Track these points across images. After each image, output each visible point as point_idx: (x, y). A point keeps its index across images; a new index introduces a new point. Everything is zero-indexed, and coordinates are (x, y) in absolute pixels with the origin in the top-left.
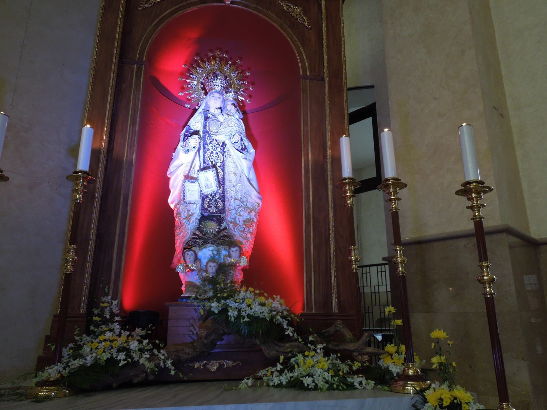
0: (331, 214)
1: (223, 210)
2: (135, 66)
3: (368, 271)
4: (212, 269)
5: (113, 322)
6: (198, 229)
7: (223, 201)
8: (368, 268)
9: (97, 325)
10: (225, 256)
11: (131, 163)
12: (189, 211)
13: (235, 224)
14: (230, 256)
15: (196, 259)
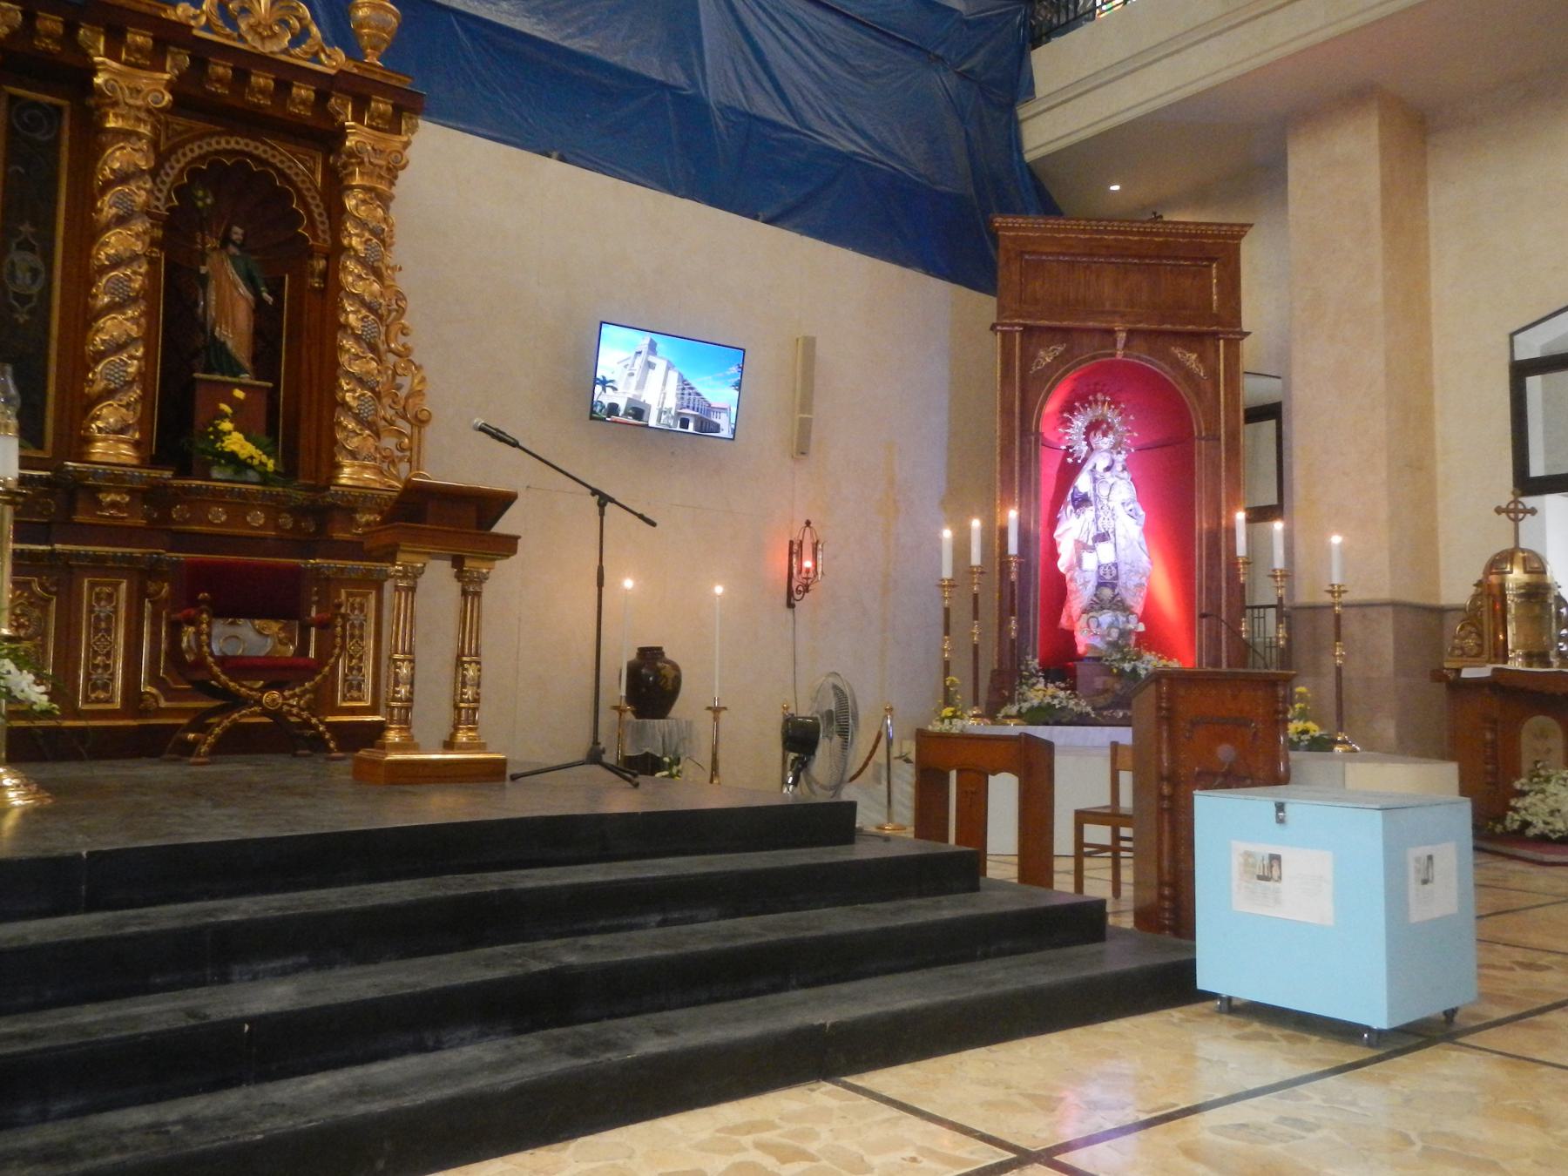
0: (1224, 585)
1: (1116, 577)
2: (1033, 438)
3: (1262, 615)
4: (1115, 633)
5: (1038, 677)
6: (1095, 595)
7: (1117, 568)
8: (1262, 610)
9: (1028, 678)
10: (1124, 623)
11: (1037, 538)
12: (1084, 578)
13: (1127, 589)
14: (1128, 622)
15: (1099, 625)
